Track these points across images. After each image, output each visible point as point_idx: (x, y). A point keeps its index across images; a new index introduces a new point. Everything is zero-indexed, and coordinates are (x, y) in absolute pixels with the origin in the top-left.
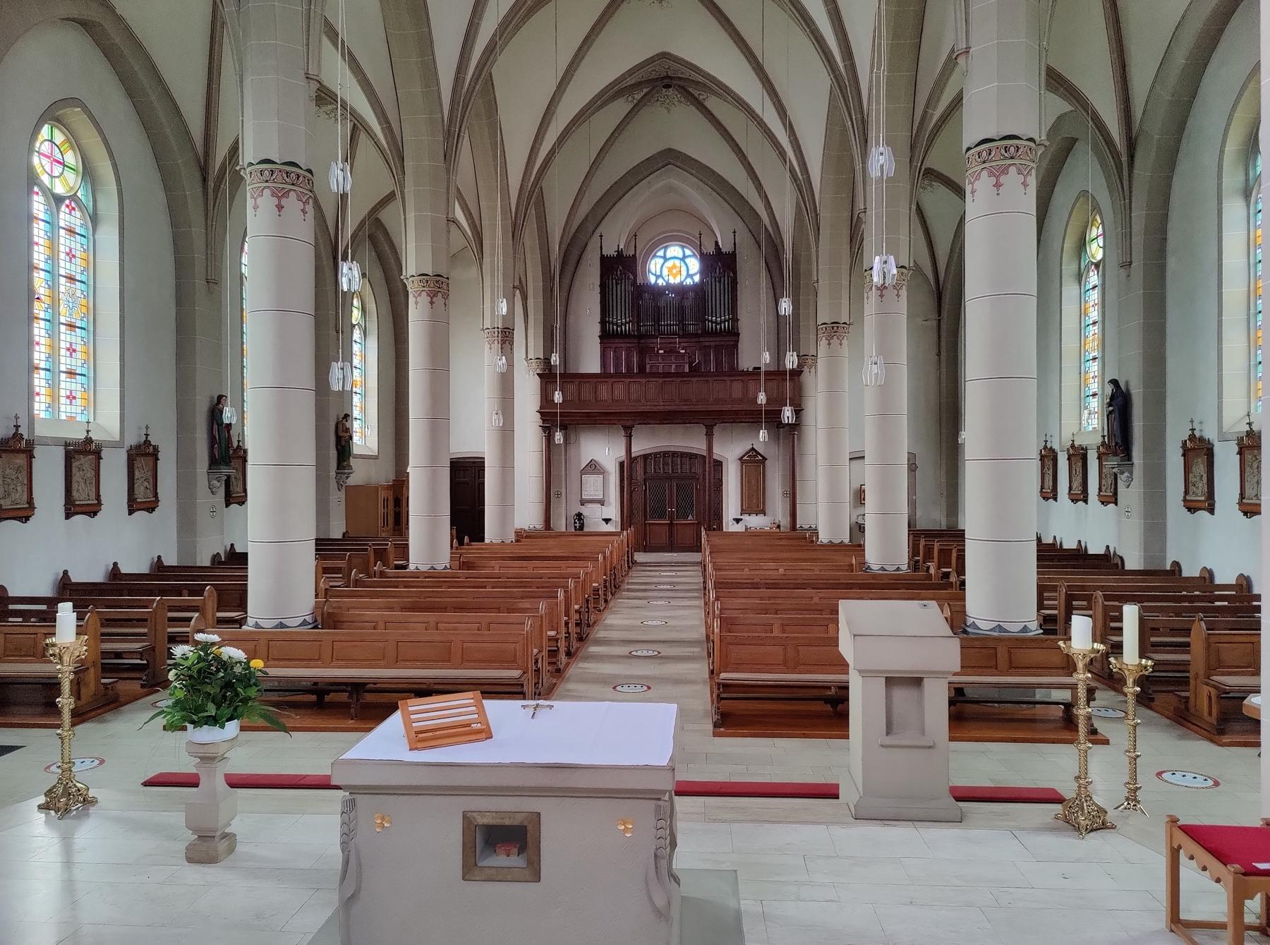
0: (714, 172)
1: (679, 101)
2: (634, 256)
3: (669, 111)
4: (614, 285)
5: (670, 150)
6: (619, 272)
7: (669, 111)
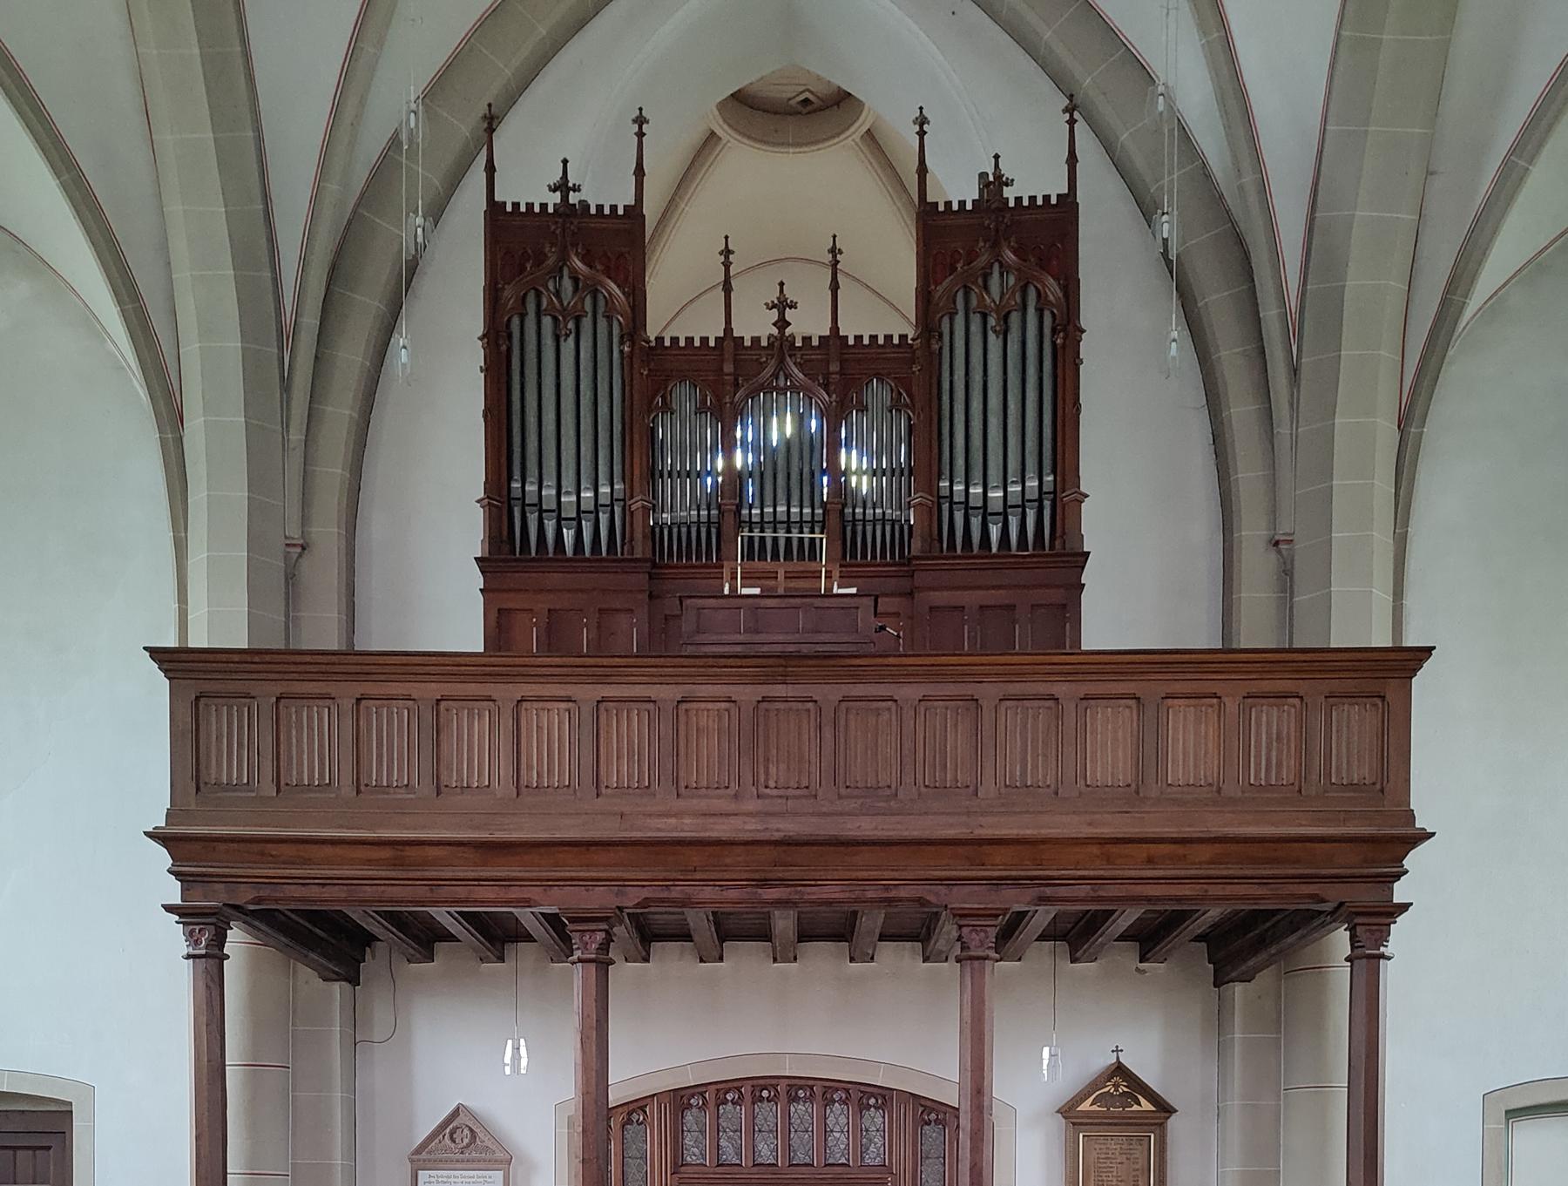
6: (567, 284)
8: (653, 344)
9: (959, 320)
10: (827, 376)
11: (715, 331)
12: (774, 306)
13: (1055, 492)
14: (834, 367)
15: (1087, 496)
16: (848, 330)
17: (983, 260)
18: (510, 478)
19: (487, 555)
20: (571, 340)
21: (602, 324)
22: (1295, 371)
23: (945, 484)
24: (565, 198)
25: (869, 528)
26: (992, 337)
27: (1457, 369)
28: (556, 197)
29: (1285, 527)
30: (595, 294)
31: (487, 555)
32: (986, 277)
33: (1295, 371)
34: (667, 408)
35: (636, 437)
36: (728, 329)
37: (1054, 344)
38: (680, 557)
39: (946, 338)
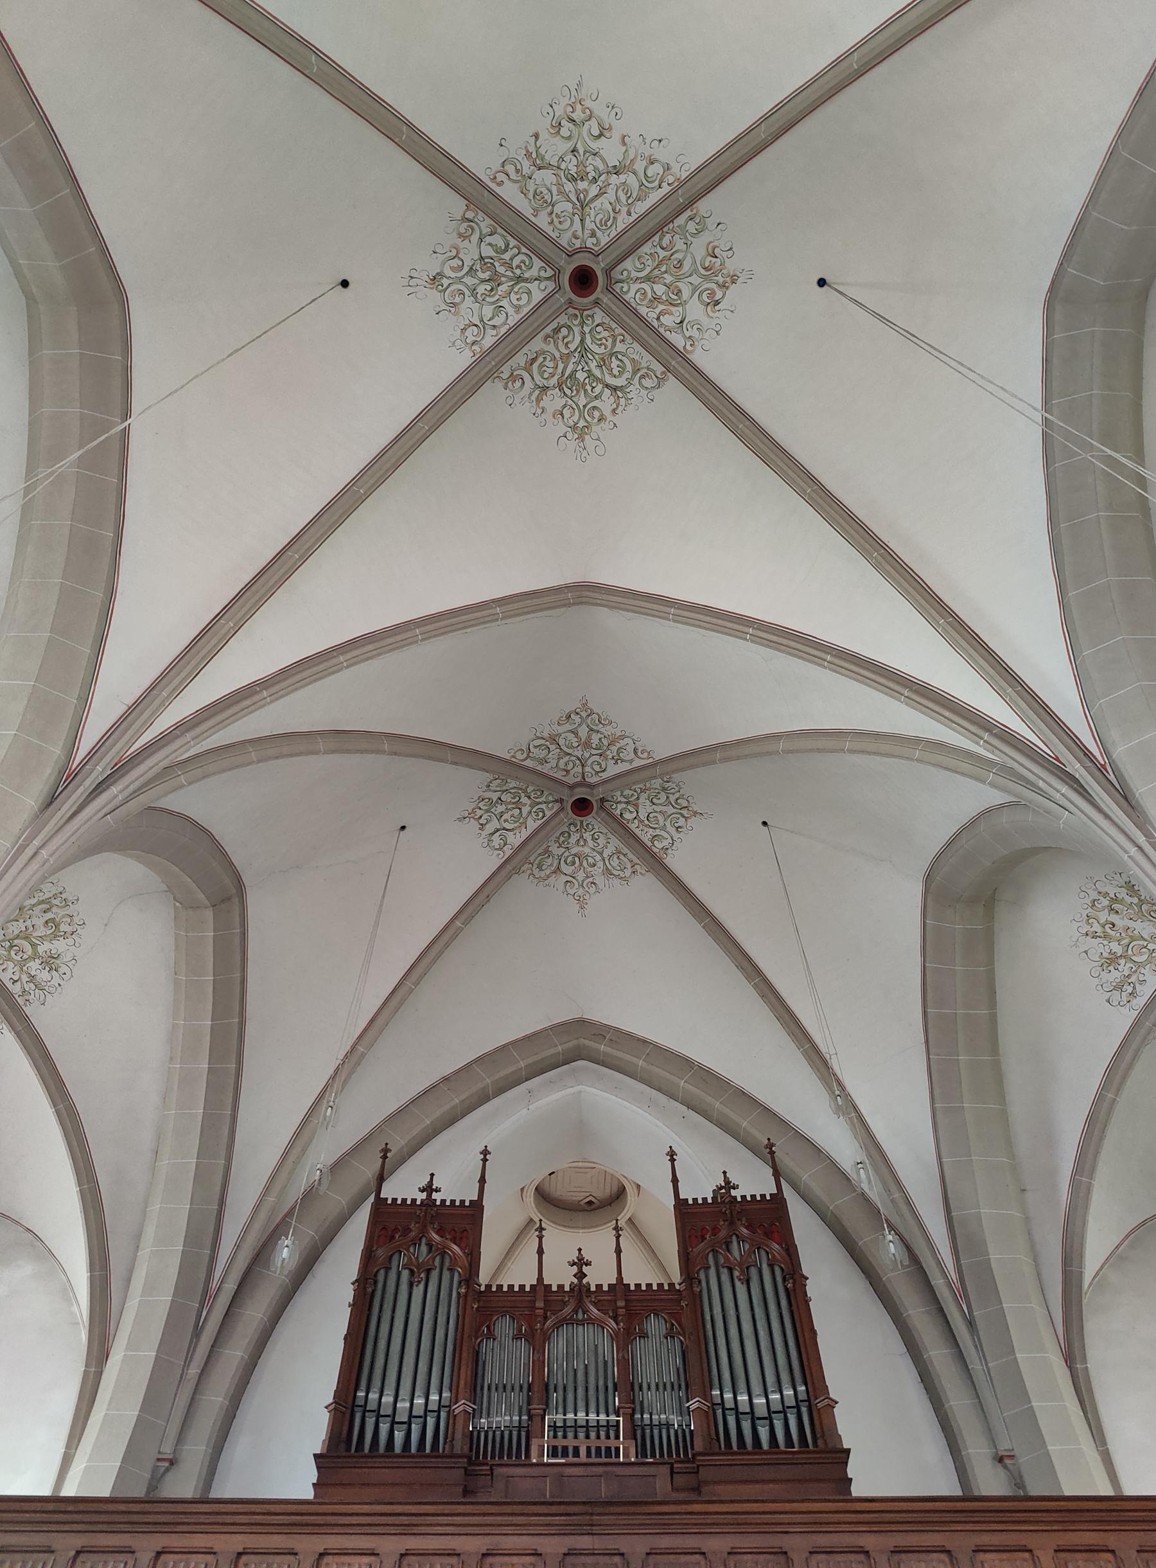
0: (686, 1064)
1: (608, 872)
2: (477, 1206)
3: (581, 902)
4: (404, 1287)
5: (581, 1024)
6: (424, 1248)
7: (581, 902)
8: (483, 1288)
9: (712, 1272)
10: (615, 1310)
11: (530, 1280)
12: (574, 1264)
13: (809, 1400)
14: (621, 1303)
15: (836, 1403)
16: (630, 1279)
17: (723, 1234)
18: (357, 1389)
19: (325, 1452)
20: (422, 1286)
21: (446, 1275)
22: (971, 1324)
23: (716, 1392)
24: (429, 1195)
25: (656, 1432)
26: (738, 1284)
27: (1093, 1325)
28: (424, 1195)
29: (1004, 1446)
30: (443, 1254)
31: (325, 1452)
32: (728, 1245)
33: (971, 1324)
34: (491, 1335)
35: (464, 1355)
36: (540, 1278)
37: (787, 1289)
38: (493, 1457)
39: (704, 1284)
